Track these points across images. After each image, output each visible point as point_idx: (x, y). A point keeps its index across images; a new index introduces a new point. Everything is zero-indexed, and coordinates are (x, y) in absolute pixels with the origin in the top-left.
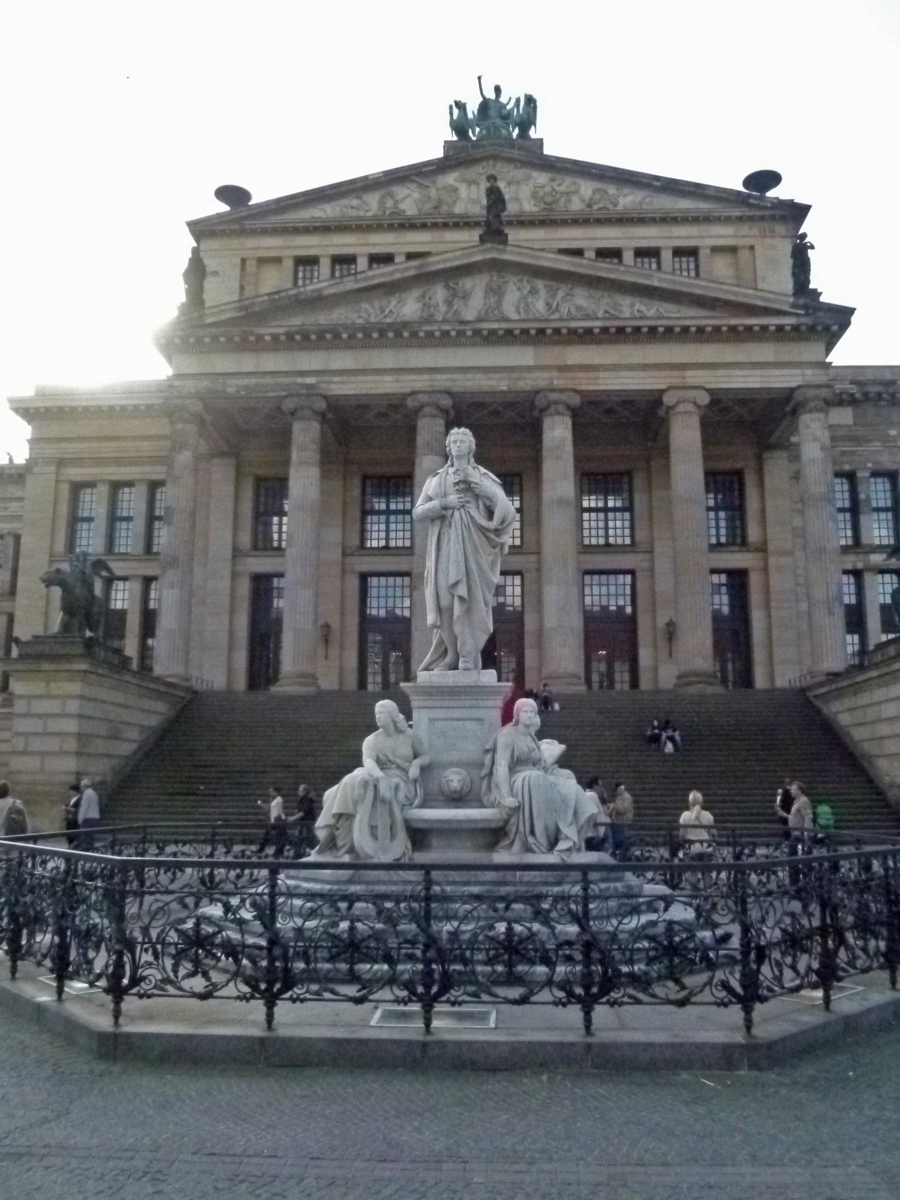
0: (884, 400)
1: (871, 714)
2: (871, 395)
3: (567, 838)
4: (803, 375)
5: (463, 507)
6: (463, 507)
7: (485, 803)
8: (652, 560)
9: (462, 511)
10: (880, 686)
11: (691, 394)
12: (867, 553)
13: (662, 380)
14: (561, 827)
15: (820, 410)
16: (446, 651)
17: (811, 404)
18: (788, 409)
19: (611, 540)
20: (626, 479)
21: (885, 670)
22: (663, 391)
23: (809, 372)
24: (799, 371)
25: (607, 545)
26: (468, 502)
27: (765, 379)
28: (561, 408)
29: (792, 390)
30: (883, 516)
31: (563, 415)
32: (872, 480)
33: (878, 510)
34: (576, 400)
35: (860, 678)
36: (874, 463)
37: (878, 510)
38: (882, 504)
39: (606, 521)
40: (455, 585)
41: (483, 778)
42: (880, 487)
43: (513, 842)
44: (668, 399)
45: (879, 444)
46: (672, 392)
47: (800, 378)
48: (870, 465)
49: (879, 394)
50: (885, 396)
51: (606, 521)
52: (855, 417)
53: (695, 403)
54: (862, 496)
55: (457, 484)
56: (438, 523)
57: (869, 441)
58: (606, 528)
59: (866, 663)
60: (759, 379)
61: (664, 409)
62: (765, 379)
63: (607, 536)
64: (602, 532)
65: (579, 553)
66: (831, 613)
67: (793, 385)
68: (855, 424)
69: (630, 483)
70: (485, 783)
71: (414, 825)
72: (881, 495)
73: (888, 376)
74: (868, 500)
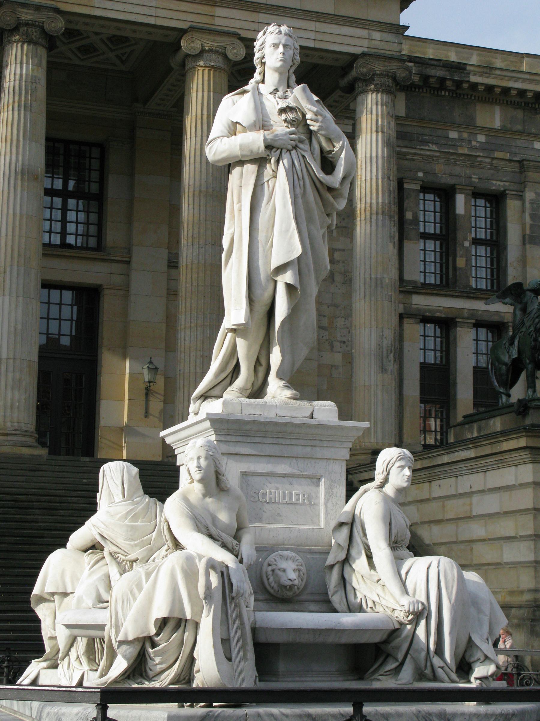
0: (446, 90)
1: (454, 508)
2: (432, 80)
3: (486, 657)
4: (370, 39)
5: (295, 147)
6: (295, 147)
7: (337, 606)
8: (128, 275)
9: (293, 152)
10: (472, 471)
11: (222, 41)
12: (410, 293)
13: (183, 16)
14: (477, 640)
15: (388, 91)
16: (237, 369)
17: (377, 80)
18: (344, 82)
19: (71, 240)
20: (96, 152)
21: (487, 450)
22: (183, 32)
23: (377, 35)
24: (364, 33)
25: (64, 245)
26: (301, 141)
27: (319, 37)
28: (34, 33)
29: (355, 57)
30: (430, 245)
31: (36, 43)
32: (421, 196)
33: (425, 236)
34: (57, 25)
35: (446, 459)
36: (425, 173)
37: (425, 236)
38: (430, 229)
39: (64, 210)
40: (281, 269)
41: (332, 567)
42: (430, 206)
43: (402, 664)
44: (188, 45)
45: (434, 147)
46: (196, 35)
47: (365, 43)
48: (420, 174)
49: (442, 81)
50: (449, 83)
51: (64, 210)
52: (407, 107)
53: (225, 56)
54: (409, 215)
55: (282, 111)
56: (250, 169)
57: (426, 143)
58: (64, 221)
59: (451, 440)
60: (312, 35)
61: (179, 57)
62: (319, 37)
63: (64, 233)
64: (57, 227)
65: (44, 255)
66: (383, 369)
67: (357, 50)
68: (407, 116)
69: (102, 159)
70: (335, 574)
71: (262, 639)
72: (430, 217)
73: (453, 57)
74: (416, 221)
